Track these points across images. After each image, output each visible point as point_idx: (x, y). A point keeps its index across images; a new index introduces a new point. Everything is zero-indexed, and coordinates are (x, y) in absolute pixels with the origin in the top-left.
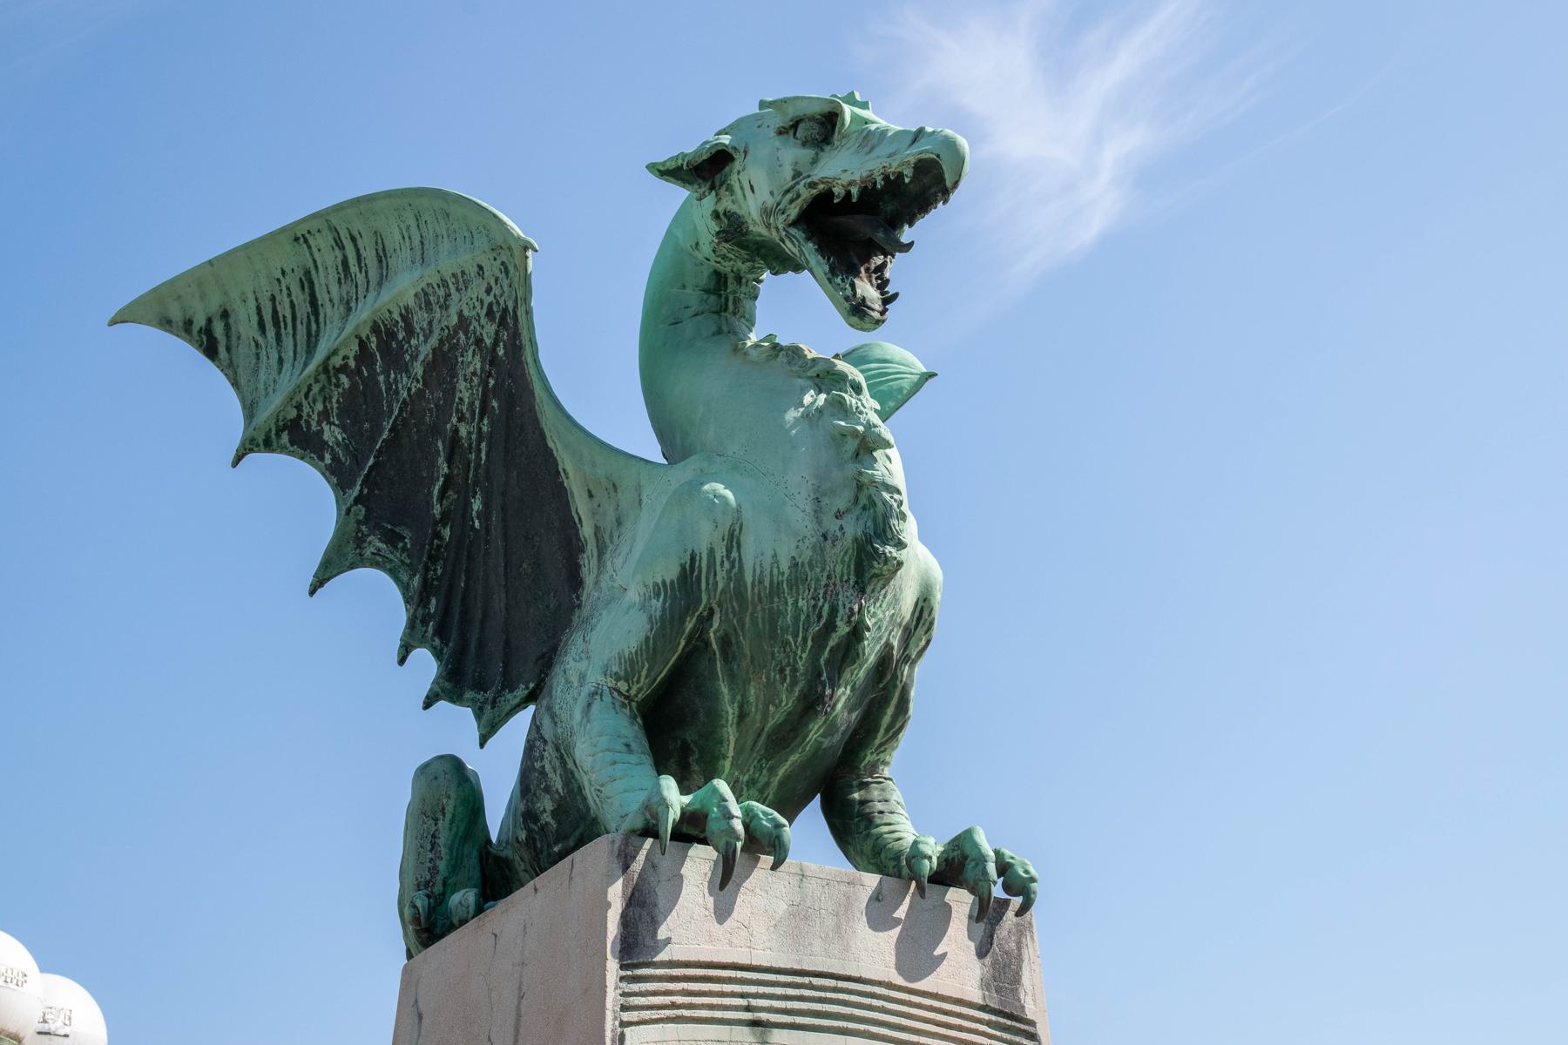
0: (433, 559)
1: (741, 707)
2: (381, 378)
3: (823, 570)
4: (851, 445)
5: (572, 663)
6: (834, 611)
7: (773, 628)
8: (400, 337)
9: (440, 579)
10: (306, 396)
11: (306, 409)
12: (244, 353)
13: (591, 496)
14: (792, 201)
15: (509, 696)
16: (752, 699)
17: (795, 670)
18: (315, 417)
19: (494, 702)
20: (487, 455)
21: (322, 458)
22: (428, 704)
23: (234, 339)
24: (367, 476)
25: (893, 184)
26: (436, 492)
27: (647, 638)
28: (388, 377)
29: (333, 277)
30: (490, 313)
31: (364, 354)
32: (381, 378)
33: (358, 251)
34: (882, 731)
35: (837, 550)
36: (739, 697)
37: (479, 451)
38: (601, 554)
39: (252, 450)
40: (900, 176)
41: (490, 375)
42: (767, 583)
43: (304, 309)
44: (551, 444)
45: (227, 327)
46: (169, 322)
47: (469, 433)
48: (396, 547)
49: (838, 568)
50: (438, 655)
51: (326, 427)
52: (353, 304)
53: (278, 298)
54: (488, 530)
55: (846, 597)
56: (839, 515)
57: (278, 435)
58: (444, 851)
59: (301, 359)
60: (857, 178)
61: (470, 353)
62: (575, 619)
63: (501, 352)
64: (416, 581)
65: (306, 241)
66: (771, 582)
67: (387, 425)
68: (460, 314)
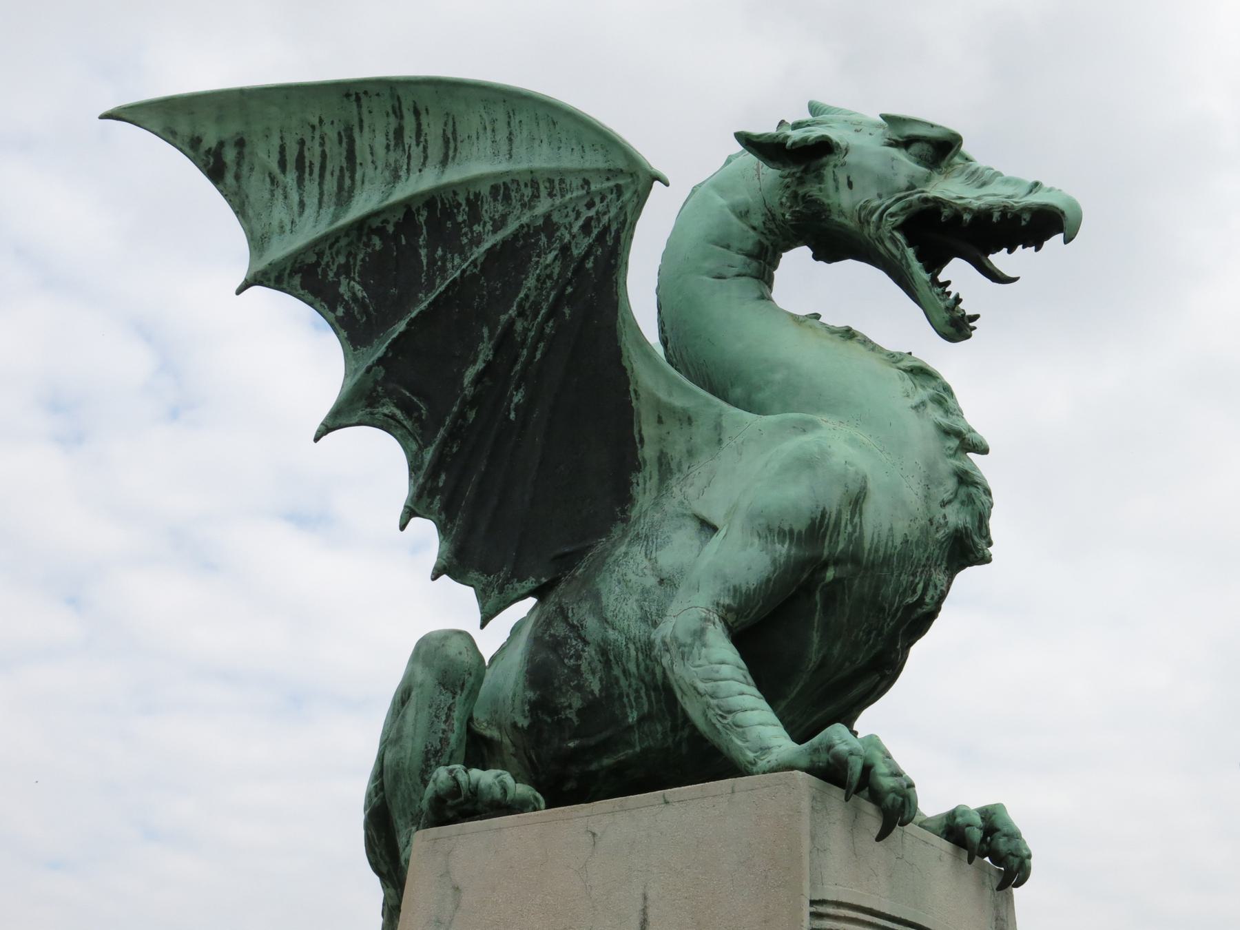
1: (824, 657)
3: (925, 551)
4: (954, 443)
8: (460, 219)
10: (331, 247)
11: (326, 259)
12: (256, 187)
13: (660, 421)
14: (903, 209)
15: (517, 585)
17: (879, 634)
18: (335, 268)
20: (544, 355)
22: (435, 576)
24: (395, 340)
26: (470, 373)
27: (768, 580)
29: (380, 141)
30: (586, 228)
32: (423, 252)
33: (419, 125)
37: (535, 349)
39: (261, 284)
40: (1017, 216)
41: (569, 282)
44: (625, 363)
45: (240, 157)
46: (174, 133)
49: (937, 552)
50: (443, 529)
52: (403, 173)
53: (308, 144)
55: (939, 577)
57: (291, 276)
58: (456, 725)
60: (976, 204)
61: (550, 257)
62: (617, 531)
64: (429, 454)
65: (358, 99)
66: (885, 552)
68: (548, 217)
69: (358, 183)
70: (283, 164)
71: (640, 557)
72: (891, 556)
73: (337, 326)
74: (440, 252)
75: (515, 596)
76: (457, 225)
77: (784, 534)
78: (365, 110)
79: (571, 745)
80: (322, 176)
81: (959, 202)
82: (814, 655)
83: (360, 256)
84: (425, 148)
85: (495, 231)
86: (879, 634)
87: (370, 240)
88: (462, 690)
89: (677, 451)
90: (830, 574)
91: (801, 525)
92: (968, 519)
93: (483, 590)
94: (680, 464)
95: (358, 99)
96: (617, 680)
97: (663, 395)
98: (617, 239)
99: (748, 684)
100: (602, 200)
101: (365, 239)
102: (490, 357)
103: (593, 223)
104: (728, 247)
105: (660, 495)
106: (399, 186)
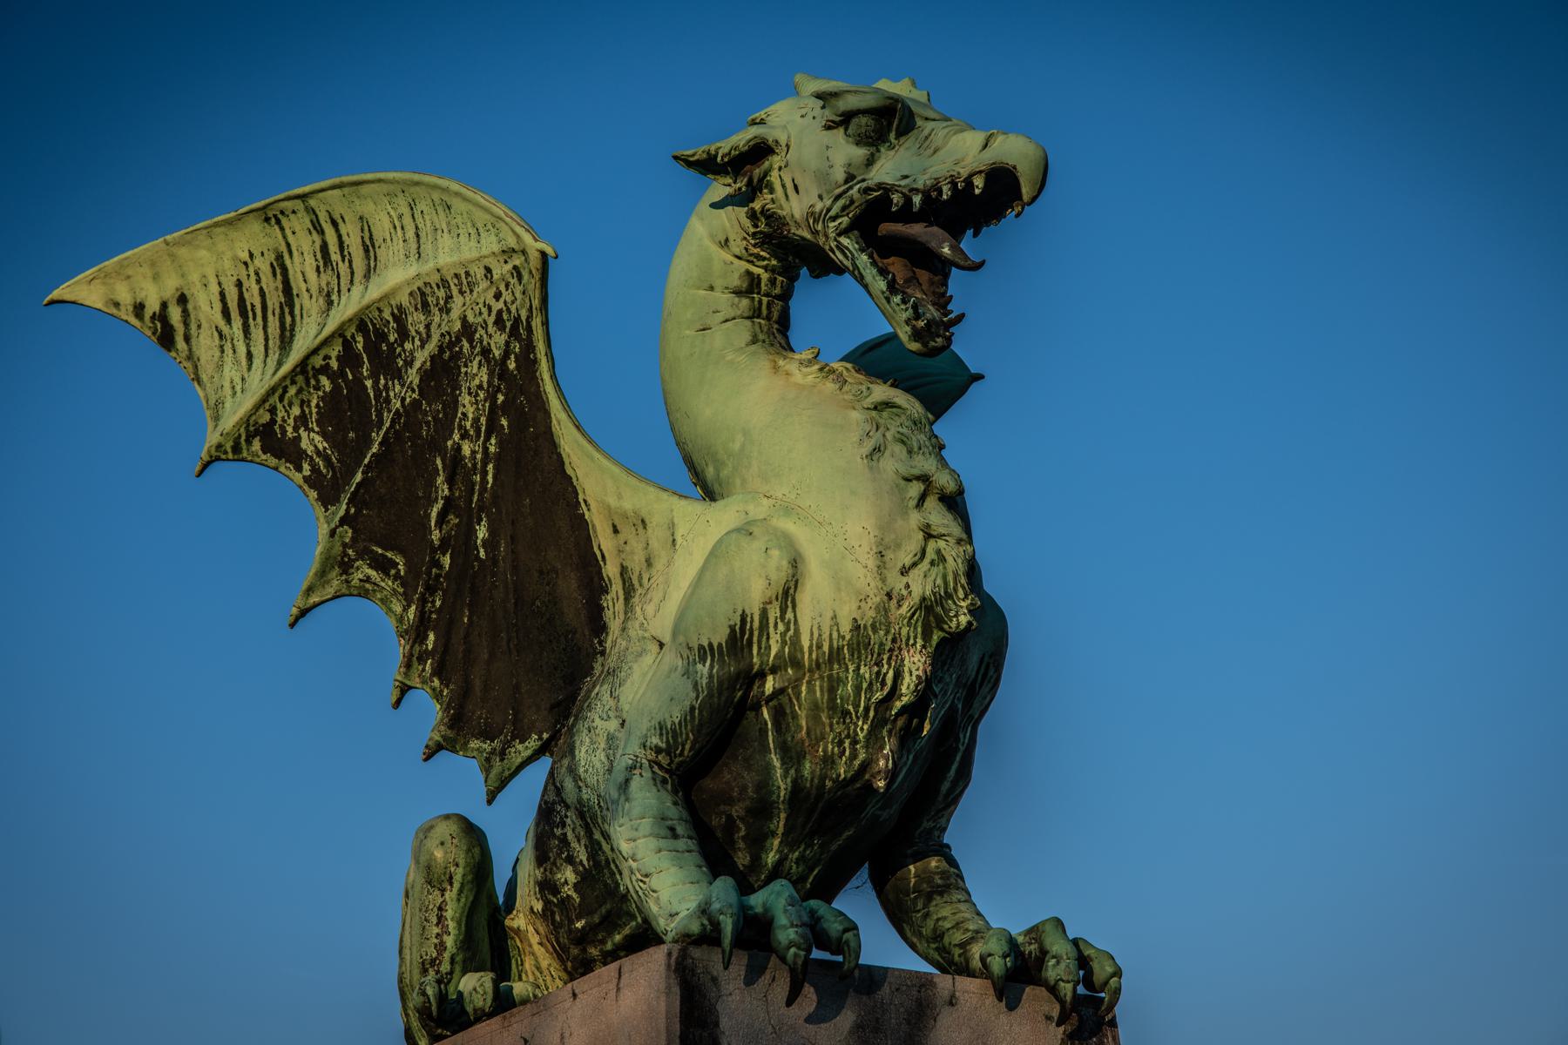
0: (431, 589)
1: (795, 782)
2: (369, 383)
3: (887, 632)
4: (916, 489)
5: (598, 722)
6: (898, 676)
7: (832, 699)
9: (439, 611)
10: (281, 399)
11: (281, 414)
13: (616, 531)
14: (844, 208)
15: (520, 747)
16: (806, 773)
17: (855, 742)
18: (291, 421)
19: (503, 755)
20: (495, 478)
21: (299, 469)
23: (193, 327)
24: (354, 494)
25: (963, 191)
26: (434, 514)
27: (692, 708)
28: (376, 383)
29: (310, 265)
30: (499, 322)
31: (349, 357)
32: (369, 383)
33: (340, 237)
34: (940, 798)
35: (904, 610)
36: (792, 772)
37: (484, 473)
38: (628, 597)
39: (218, 459)
41: (499, 390)
42: (826, 648)
43: (275, 299)
44: (569, 471)
46: (117, 305)
47: (474, 452)
48: (387, 574)
49: (904, 631)
50: (437, 696)
51: (304, 434)
52: (334, 297)
54: (495, 562)
56: (904, 571)
57: (249, 442)
58: (452, 925)
59: (274, 357)
61: (475, 363)
63: (512, 365)
65: (278, 222)
66: (831, 647)
67: (377, 437)
68: (464, 319)
69: (298, 318)
70: (226, 313)
71: (606, 697)
72: (840, 649)
73: (306, 487)
74: (382, 381)
75: (519, 760)
76: (391, 346)
77: (703, 653)
78: (289, 233)
79: (579, 925)
80: (265, 318)
81: (903, 183)
82: (781, 783)
83: (314, 403)
84: (350, 262)
85: (422, 347)
86: (855, 742)
87: (318, 381)
88: (451, 884)
89: (636, 563)
90: (770, 685)
91: (720, 637)
92: (939, 581)
93: (488, 760)
94: (640, 578)
95: (278, 222)
96: (599, 844)
97: (612, 501)
98: (529, 329)
99: (675, 836)
100: (507, 286)
101: (313, 382)
102: (446, 492)
103: (505, 317)
104: (712, 288)
105: (626, 620)
106: (332, 313)
